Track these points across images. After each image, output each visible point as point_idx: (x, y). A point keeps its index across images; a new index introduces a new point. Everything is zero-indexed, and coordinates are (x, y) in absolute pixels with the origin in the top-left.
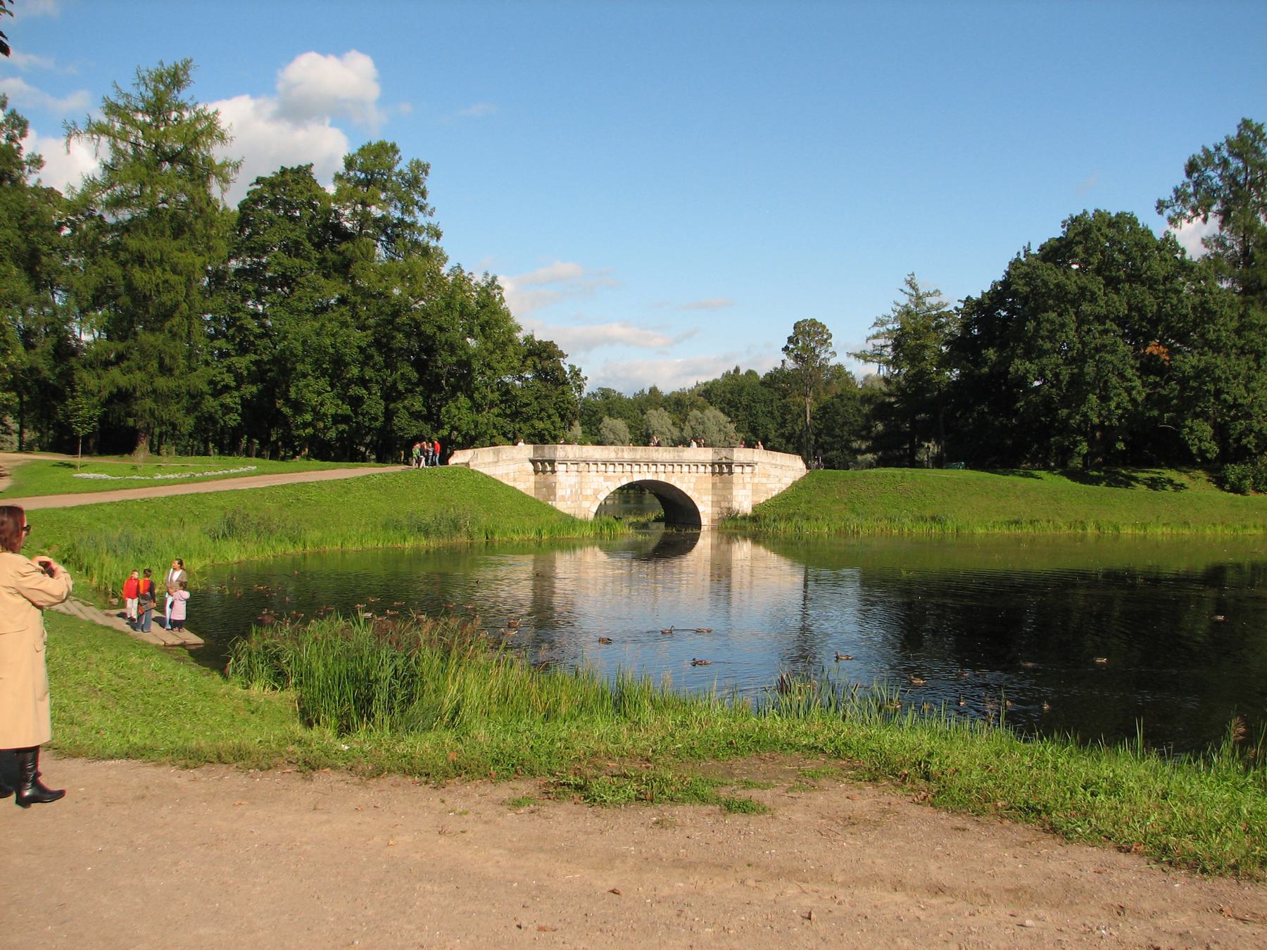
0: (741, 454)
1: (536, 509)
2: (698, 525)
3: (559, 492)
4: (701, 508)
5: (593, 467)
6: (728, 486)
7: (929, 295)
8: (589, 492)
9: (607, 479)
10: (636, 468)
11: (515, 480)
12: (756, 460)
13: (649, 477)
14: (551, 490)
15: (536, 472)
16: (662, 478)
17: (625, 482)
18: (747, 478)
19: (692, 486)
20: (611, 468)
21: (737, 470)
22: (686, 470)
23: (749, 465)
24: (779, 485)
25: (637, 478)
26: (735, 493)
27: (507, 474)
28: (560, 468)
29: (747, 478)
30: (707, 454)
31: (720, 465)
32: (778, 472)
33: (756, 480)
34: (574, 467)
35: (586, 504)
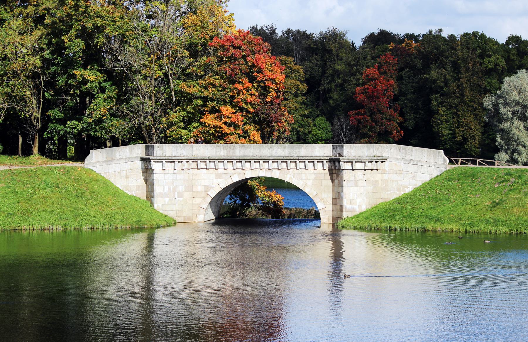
5: (202, 165)
8: (200, 189)
9: (218, 176)
10: (247, 165)
11: (127, 178)
12: (385, 155)
13: (262, 174)
16: (276, 175)
17: (236, 178)
18: (359, 174)
19: (309, 183)
20: (220, 165)
23: (359, 161)
24: (414, 182)
25: (249, 174)
26: (345, 189)
27: (120, 172)
29: (359, 174)
30: (325, 150)
32: (412, 168)
33: (386, 177)
34: (171, 165)
35: (198, 200)
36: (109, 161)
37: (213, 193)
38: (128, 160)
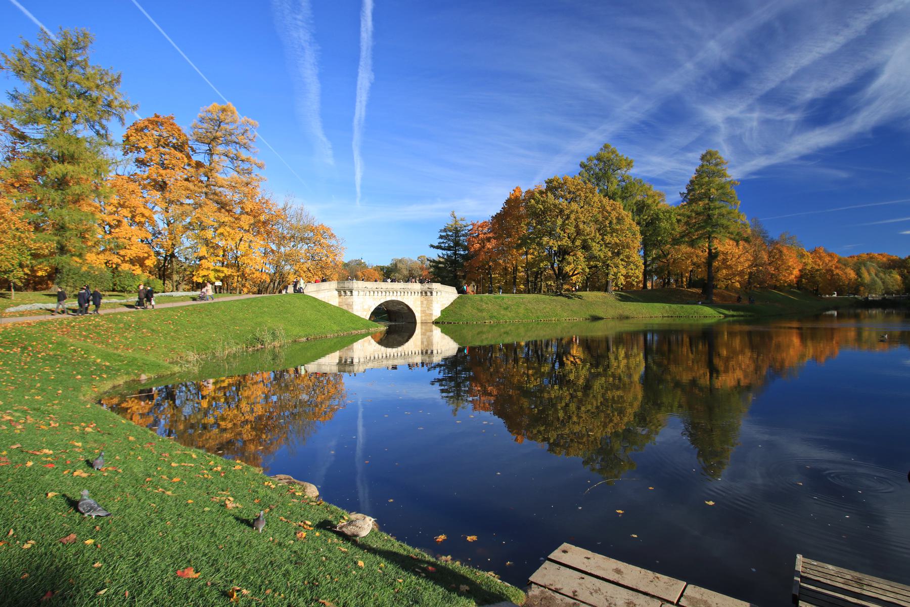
0: (436, 286)
1: (343, 315)
2: (415, 323)
3: (355, 307)
4: (416, 314)
6: (430, 303)
7: (462, 220)
8: (366, 307)
14: (350, 305)
15: (340, 296)
16: (399, 299)
17: (382, 301)
21: (434, 294)
22: (409, 295)
28: (355, 293)
31: (426, 293)
34: (361, 293)
36: (317, 291)
37: (372, 310)
38: (329, 290)
